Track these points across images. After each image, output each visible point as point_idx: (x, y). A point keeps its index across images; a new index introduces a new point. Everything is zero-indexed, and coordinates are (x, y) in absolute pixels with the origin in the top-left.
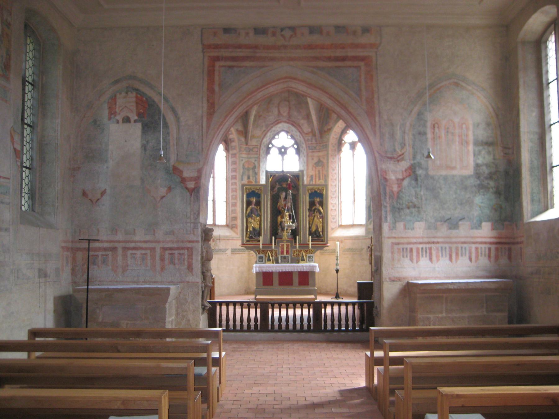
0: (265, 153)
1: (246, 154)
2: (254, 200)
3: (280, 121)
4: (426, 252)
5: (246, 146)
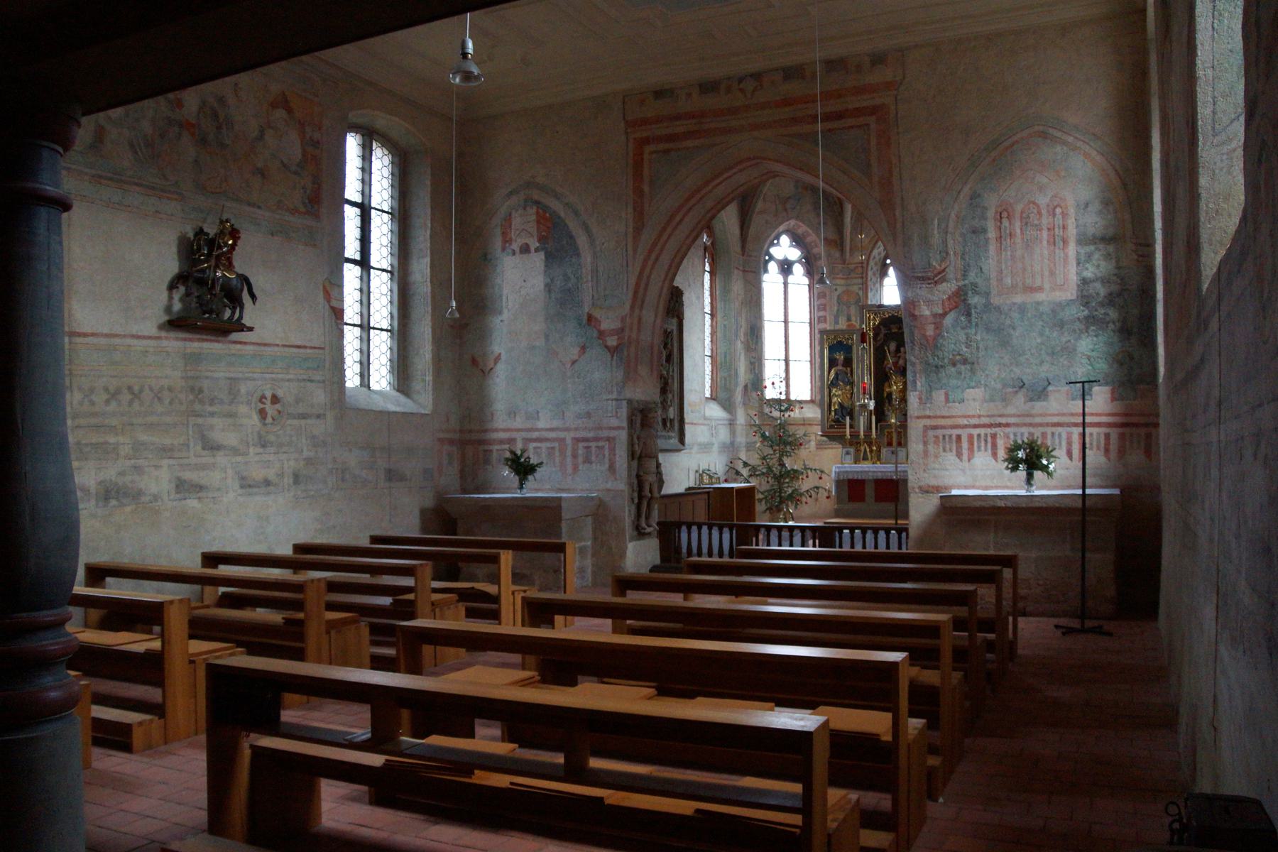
0: (878, 275)
1: (843, 279)
2: (840, 357)
4: (986, 441)
5: (843, 266)
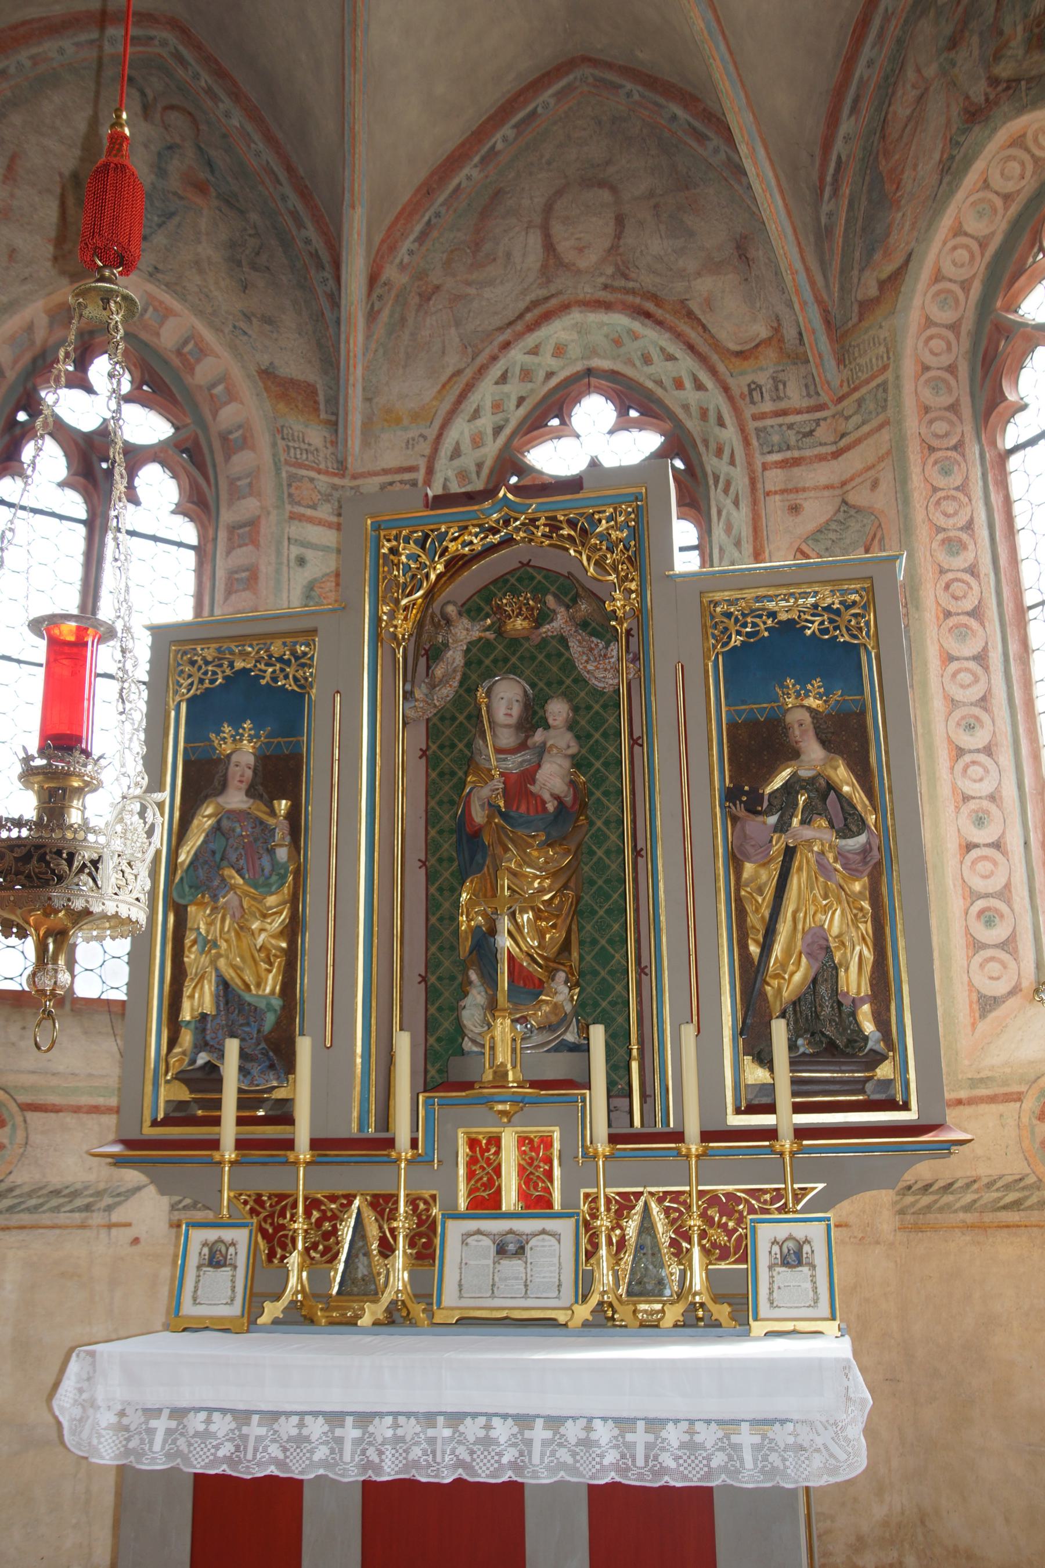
3: (554, 302)
5: (337, 481)
